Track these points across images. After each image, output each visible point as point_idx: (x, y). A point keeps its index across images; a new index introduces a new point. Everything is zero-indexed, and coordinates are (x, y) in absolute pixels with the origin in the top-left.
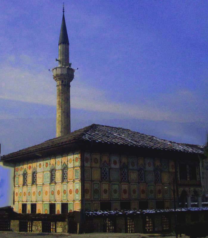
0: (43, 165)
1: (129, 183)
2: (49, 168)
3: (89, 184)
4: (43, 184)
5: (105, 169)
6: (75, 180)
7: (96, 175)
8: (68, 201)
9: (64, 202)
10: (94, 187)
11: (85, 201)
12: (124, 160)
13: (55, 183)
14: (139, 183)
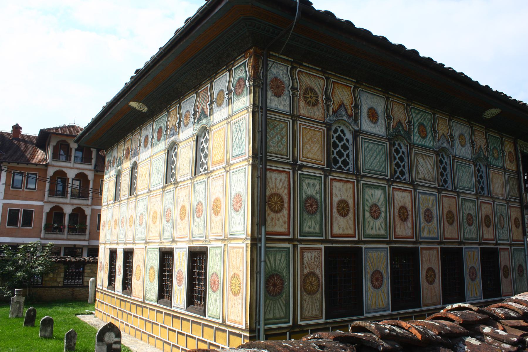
0: (153, 137)
2: (163, 145)
3: (284, 176)
4: (150, 191)
5: (342, 131)
6: (231, 162)
8: (207, 240)
11: (267, 240)
12: (399, 113)
13: (176, 183)
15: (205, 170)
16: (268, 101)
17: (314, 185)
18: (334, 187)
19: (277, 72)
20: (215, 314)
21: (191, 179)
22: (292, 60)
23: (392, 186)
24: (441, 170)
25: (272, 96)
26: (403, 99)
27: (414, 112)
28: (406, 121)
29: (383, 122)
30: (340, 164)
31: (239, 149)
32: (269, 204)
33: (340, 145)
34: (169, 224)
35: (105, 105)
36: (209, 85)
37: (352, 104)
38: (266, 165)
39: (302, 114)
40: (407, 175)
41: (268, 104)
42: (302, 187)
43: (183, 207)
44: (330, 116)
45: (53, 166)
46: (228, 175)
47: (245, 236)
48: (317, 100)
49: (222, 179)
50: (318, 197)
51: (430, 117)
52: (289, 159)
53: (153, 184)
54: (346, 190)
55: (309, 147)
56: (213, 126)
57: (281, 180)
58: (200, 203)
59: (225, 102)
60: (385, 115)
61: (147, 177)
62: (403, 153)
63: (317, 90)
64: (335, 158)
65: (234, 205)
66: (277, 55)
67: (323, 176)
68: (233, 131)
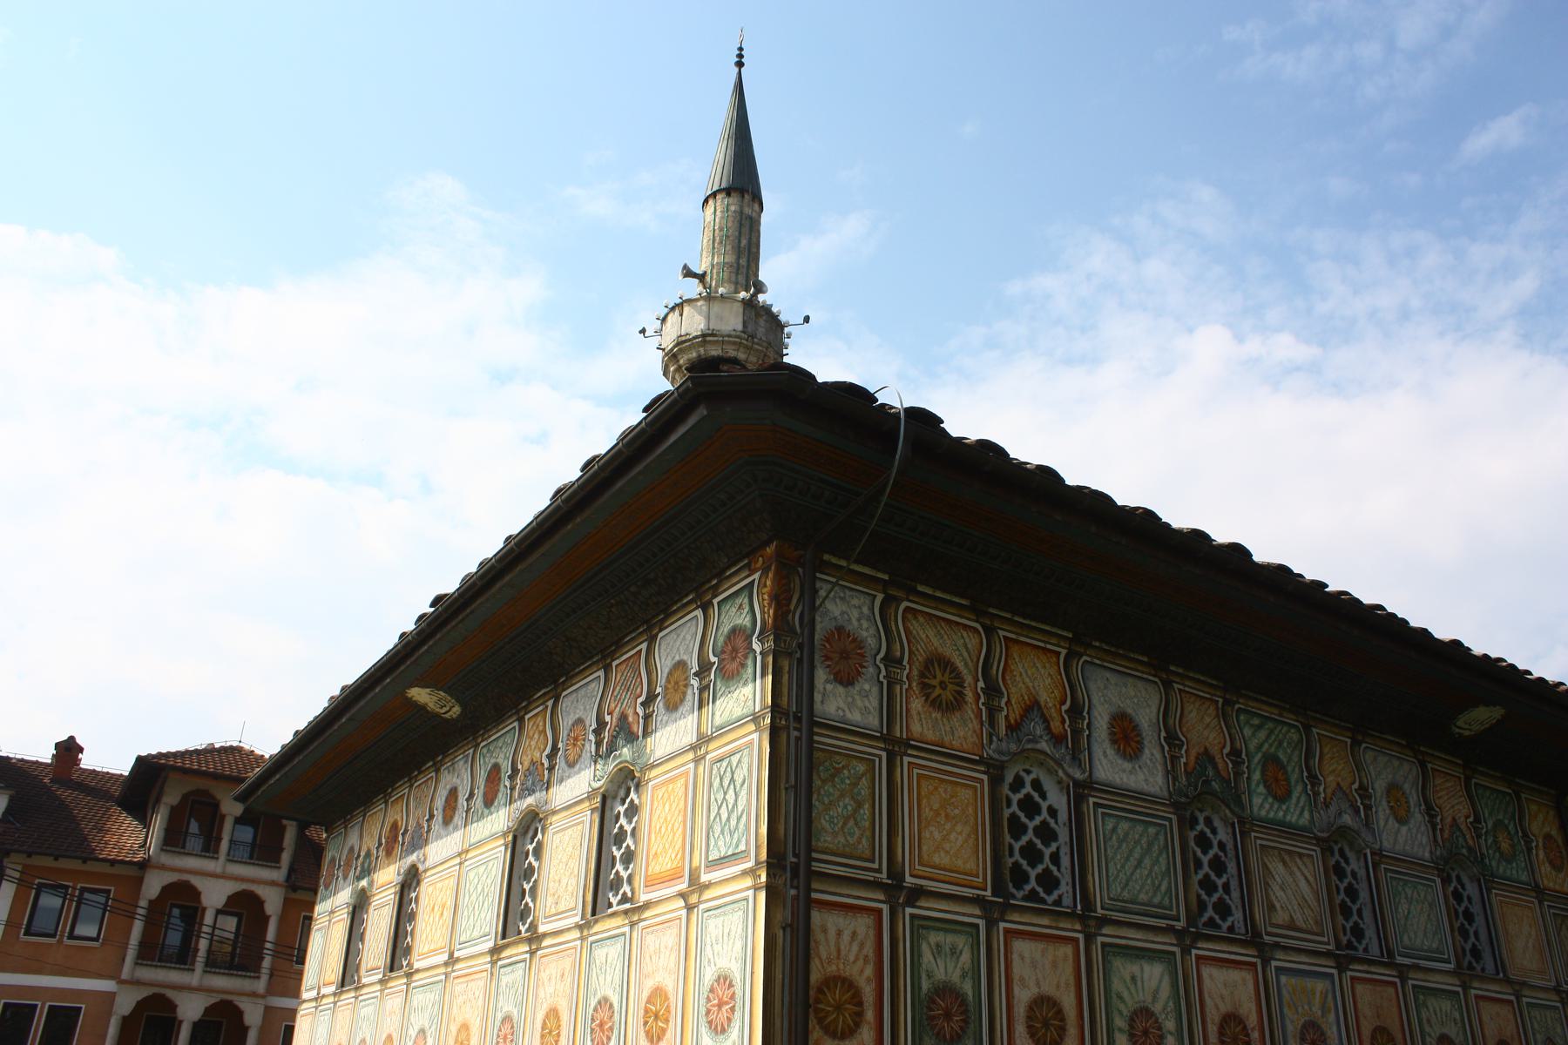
0: (471, 795)
1: (1265, 951)
2: (500, 820)
3: (863, 924)
4: (452, 960)
5: (1037, 785)
6: (704, 878)
7: (949, 840)
10: (927, 956)
12: (1203, 728)
13: (535, 938)
14: (1342, 964)
15: (625, 899)
16: (818, 697)
17: (954, 951)
18: (1015, 956)
19: (843, 613)
21: (580, 927)
22: (886, 577)
23: (1194, 952)
24: (1342, 895)
25: (827, 681)
26: (1211, 685)
27: (1247, 722)
28: (1226, 750)
29: (1158, 756)
30: (1033, 883)
32: (817, 1011)
33: (1031, 825)
35: (337, 692)
36: (644, 646)
37: (1063, 702)
38: (809, 890)
39: (916, 735)
40: (1237, 915)
41: (818, 706)
42: (920, 956)
43: (553, 1013)
44: (1000, 740)
45: (163, 868)
46: (694, 918)
48: (960, 694)
49: (675, 931)
50: (968, 988)
51: (1295, 737)
52: (879, 871)
54: (1054, 965)
55: (937, 835)
56: (653, 766)
57: (854, 934)
58: (604, 1002)
59: (689, 697)
60: (1163, 734)
61: (448, 914)
62: (1222, 846)
63: (960, 665)
64: (1016, 864)
65: (708, 1012)
66: (843, 563)
67: (981, 923)
68: (711, 785)
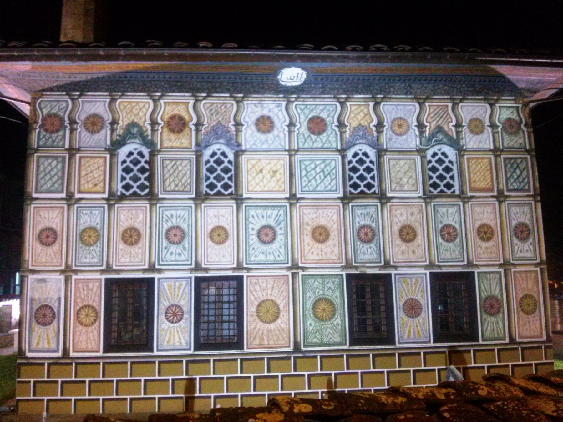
4: (293, 198)
6: (506, 194)
8: (470, 264)
9: (444, 270)
13: (383, 198)
20: (496, 336)
21: (424, 199)
31: (518, 184)
34: (372, 245)
36: (450, 105)
47: (538, 261)
53: (306, 189)
58: (448, 226)
65: (516, 234)
